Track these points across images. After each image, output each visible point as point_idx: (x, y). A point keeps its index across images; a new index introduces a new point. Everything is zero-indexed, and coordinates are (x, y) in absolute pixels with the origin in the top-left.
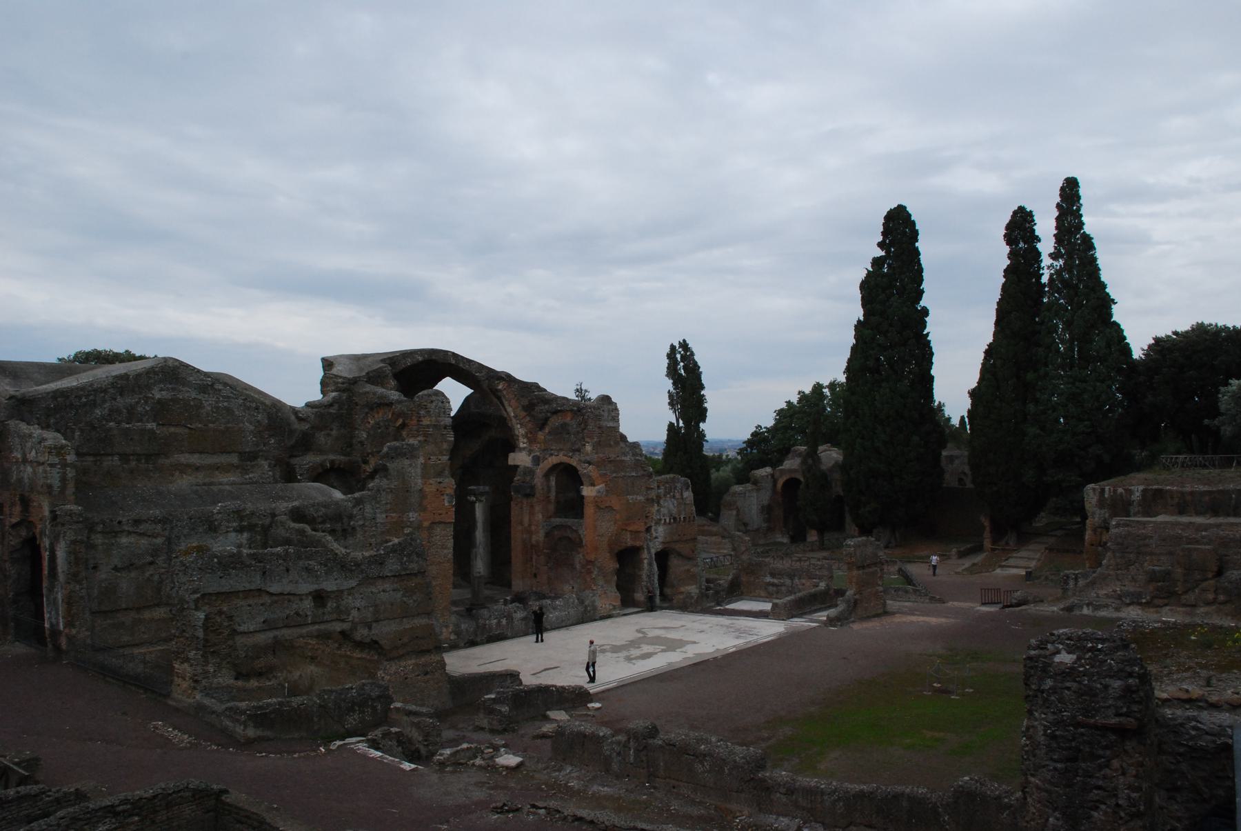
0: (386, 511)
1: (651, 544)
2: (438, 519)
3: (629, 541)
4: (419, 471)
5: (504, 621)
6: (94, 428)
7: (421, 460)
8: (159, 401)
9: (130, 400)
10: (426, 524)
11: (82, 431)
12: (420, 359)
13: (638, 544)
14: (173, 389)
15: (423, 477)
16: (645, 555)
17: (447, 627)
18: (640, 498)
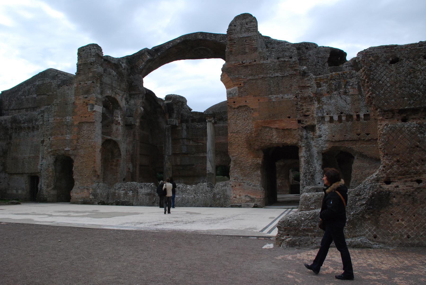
0: (54, 116)
1: (313, 143)
2: (84, 120)
3: (275, 139)
4: (73, 91)
5: (130, 193)
6: (18, 99)
7: (75, 85)
8: (38, 86)
9: (29, 87)
10: (76, 123)
11: (15, 101)
12: (178, 41)
13: (289, 141)
14: (43, 80)
15: (75, 95)
16: (302, 153)
17: (87, 189)
18: (291, 96)
